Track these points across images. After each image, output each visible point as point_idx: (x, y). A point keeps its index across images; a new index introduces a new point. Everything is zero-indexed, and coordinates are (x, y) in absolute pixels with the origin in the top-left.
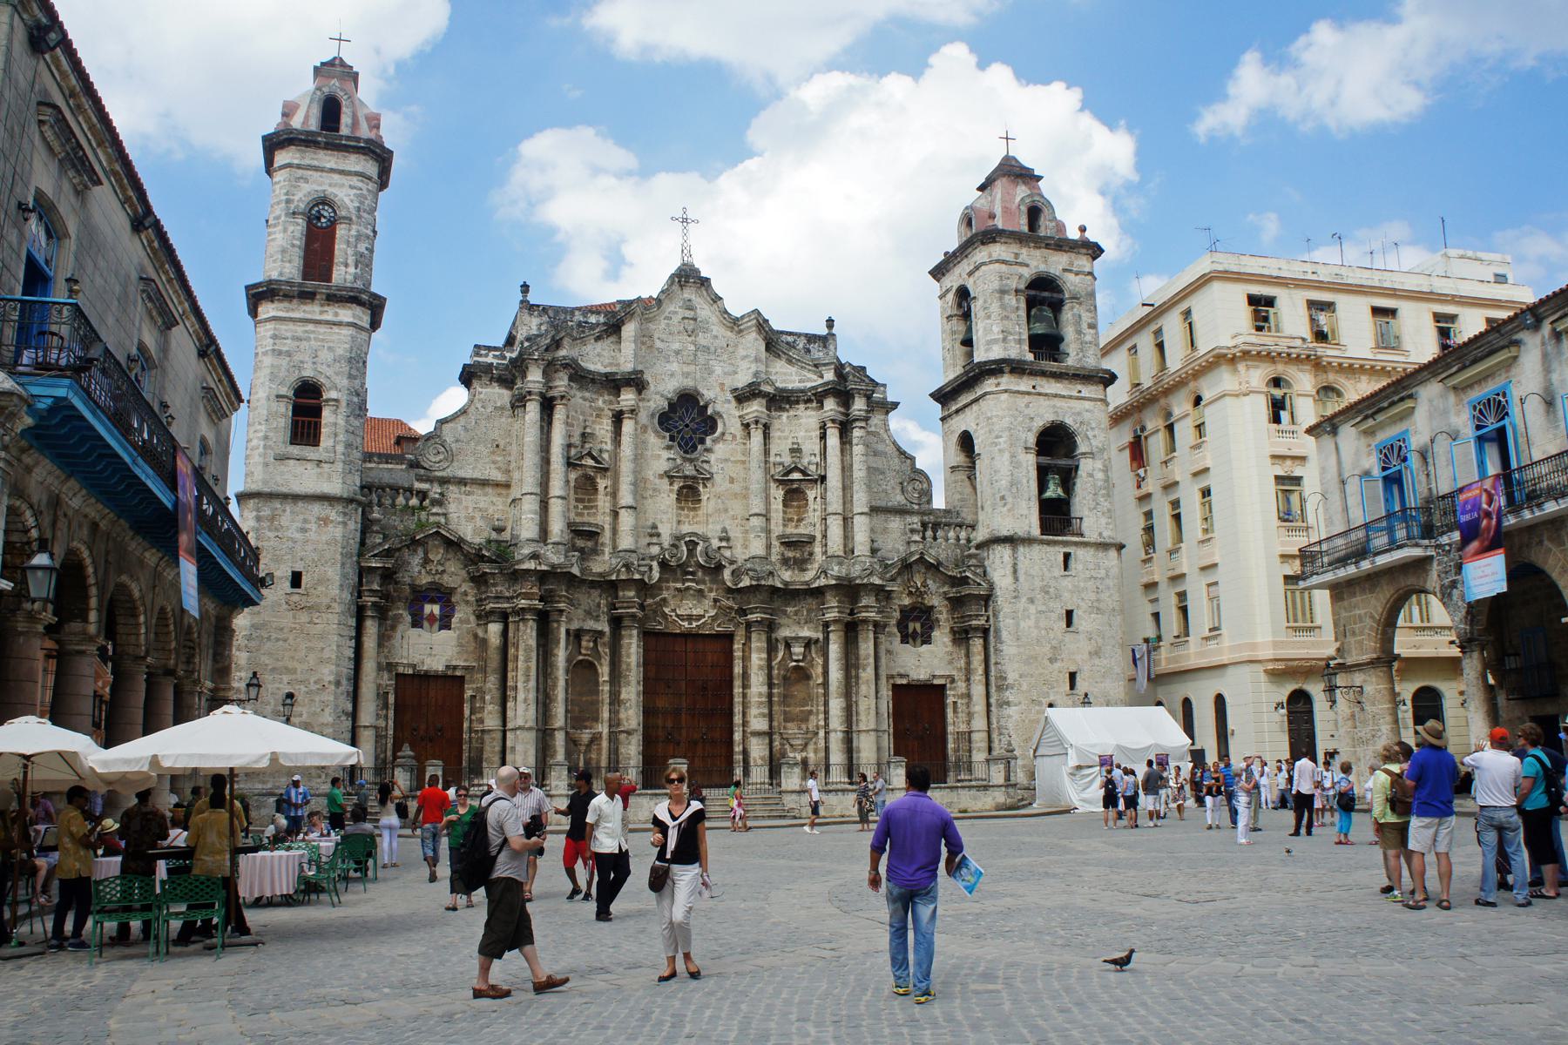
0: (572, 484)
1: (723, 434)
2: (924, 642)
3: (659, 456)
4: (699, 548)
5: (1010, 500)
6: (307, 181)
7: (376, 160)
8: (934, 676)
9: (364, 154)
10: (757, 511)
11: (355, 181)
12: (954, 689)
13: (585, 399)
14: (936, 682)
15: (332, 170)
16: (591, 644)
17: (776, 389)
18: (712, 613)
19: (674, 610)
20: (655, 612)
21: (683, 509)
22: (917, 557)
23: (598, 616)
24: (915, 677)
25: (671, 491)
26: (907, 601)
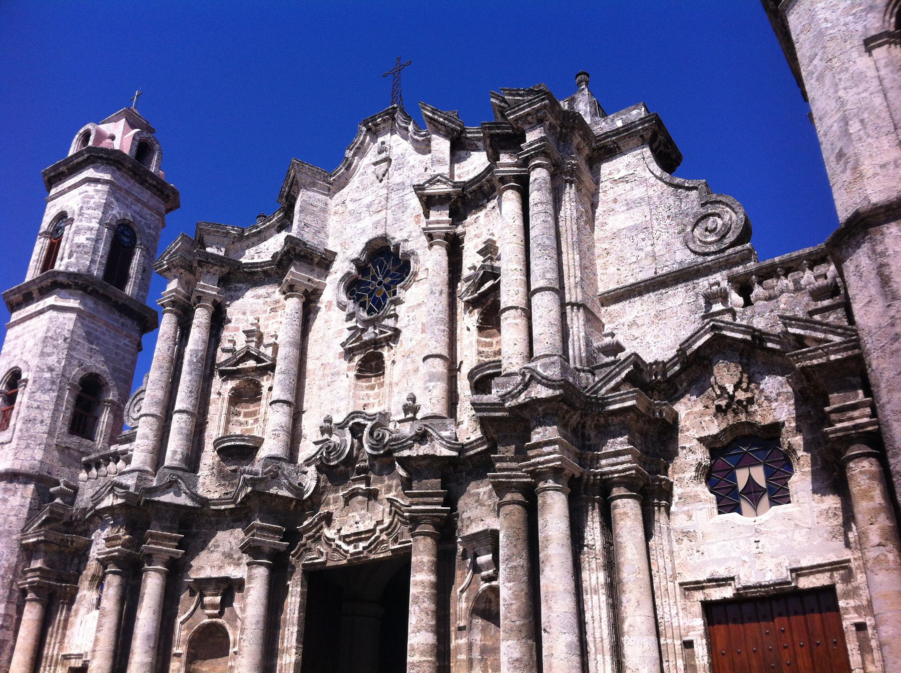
0: (226, 396)
1: (416, 274)
2: (774, 502)
3: (341, 331)
4: (366, 431)
5: (849, 151)
6: (54, 205)
7: (108, 164)
8: (798, 572)
9: (93, 162)
10: (427, 353)
11: (84, 187)
12: (853, 593)
13: (259, 297)
14: (805, 583)
15: (71, 188)
16: (218, 599)
17: (456, 184)
18: (387, 522)
19: (339, 531)
20: (317, 539)
21: (372, 388)
22: (707, 337)
23: (239, 559)
24: (752, 581)
25: (349, 369)
26: (714, 428)
